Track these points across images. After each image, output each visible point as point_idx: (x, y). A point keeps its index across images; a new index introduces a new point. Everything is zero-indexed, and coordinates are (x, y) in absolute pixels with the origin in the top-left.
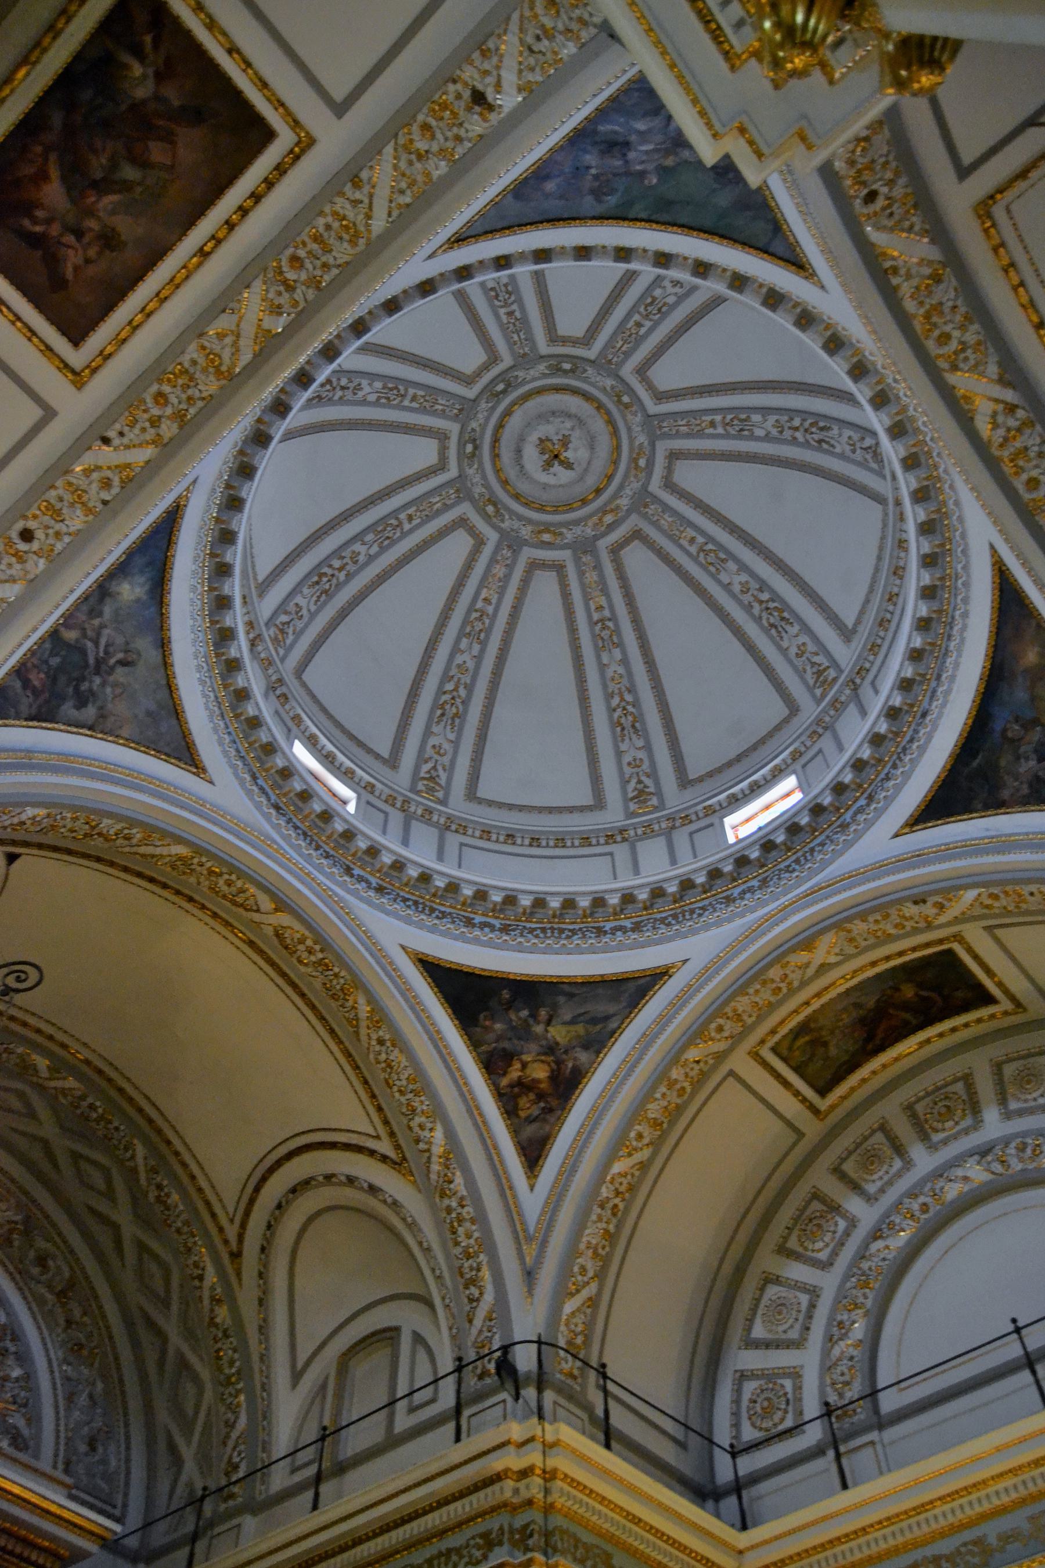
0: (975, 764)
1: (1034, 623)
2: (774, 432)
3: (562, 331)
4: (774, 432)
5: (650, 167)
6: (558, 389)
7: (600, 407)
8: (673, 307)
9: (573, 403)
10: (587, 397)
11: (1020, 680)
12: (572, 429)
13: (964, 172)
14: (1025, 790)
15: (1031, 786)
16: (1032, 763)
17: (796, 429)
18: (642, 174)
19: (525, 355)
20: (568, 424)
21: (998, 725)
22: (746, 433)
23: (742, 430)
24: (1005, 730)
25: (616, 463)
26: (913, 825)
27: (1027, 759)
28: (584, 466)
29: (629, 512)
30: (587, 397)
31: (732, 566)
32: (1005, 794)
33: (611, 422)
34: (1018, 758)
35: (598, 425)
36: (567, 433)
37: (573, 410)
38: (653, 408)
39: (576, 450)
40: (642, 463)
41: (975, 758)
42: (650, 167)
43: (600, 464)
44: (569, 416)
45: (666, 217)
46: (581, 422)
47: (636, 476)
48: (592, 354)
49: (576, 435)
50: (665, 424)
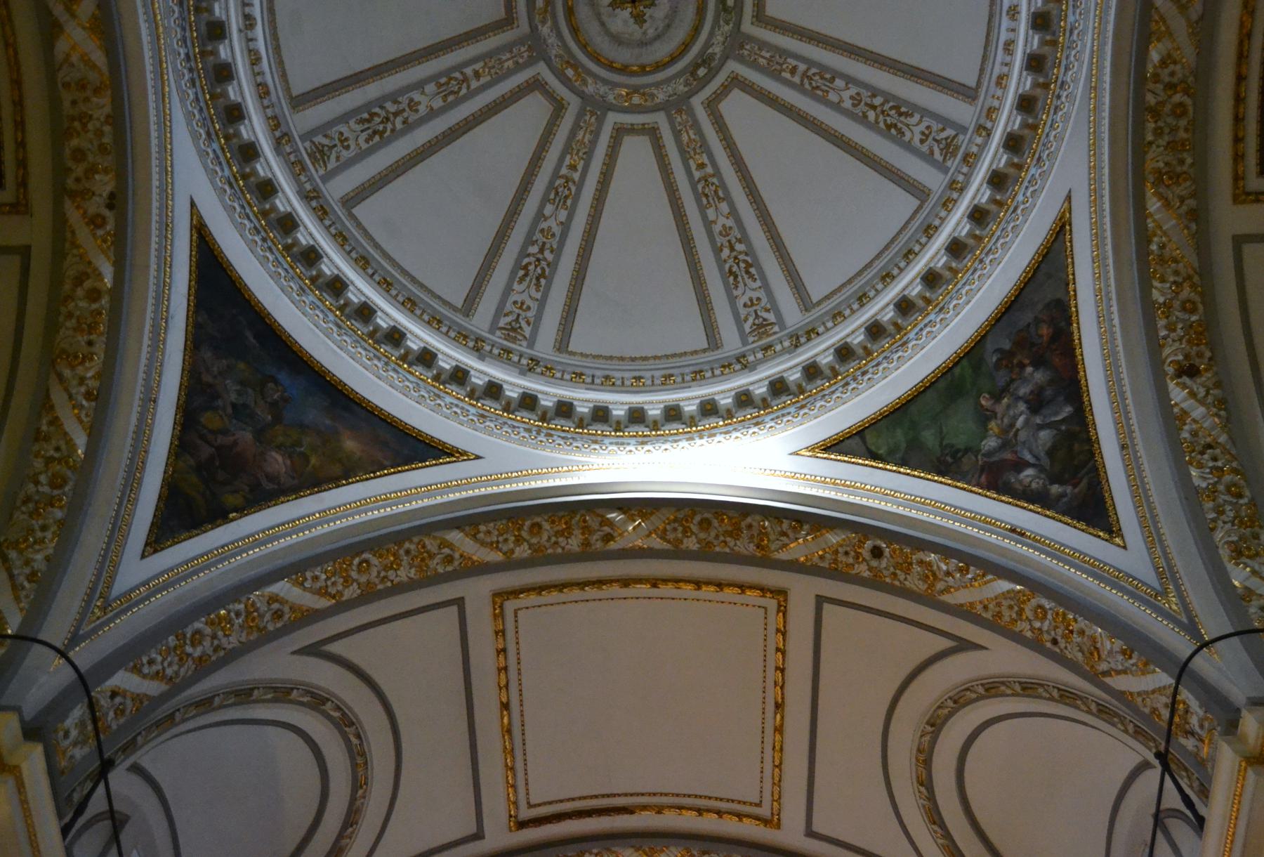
0: (249, 335)
1: (386, 463)
2: (544, 225)
3: (736, 94)
4: (544, 225)
5: (1000, 409)
6: (686, 47)
7: (643, 70)
8: (702, 210)
9: (662, 50)
10: (659, 66)
11: (328, 422)
12: (645, 33)
13: (821, 600)
14: (207, 378)
15: (210, 386)
16: (233, 397)
17: (542, 251)
18: (997, 397)
19: (742, 47)
20: (651, 32)
21: (283, 377)
22: (552, 196)
23: (557, 193)
24: (276, 382)
25: (584, 47)
26: (199, 233)
27: (239, 393)
28: (605, 18)
29: (533, 28)
30: (659, 66)
31: (438, 103)
32: (207, 354)
33: (624, 70)
34: (242, 383)
35: (623, 56)
36: (646, 26)
37: (657, 44)
38: (613, 118)
39: (625, 22)
40: (570, 72)
41: (255, 338)
42: (1000, 409)
43: (592, 30)
44: (658, 37)
45: (941, 385)
46: (643, 44)
47: (561, 57)
48: (697, 102)
49: (633, 30)
50: (593, 119)
